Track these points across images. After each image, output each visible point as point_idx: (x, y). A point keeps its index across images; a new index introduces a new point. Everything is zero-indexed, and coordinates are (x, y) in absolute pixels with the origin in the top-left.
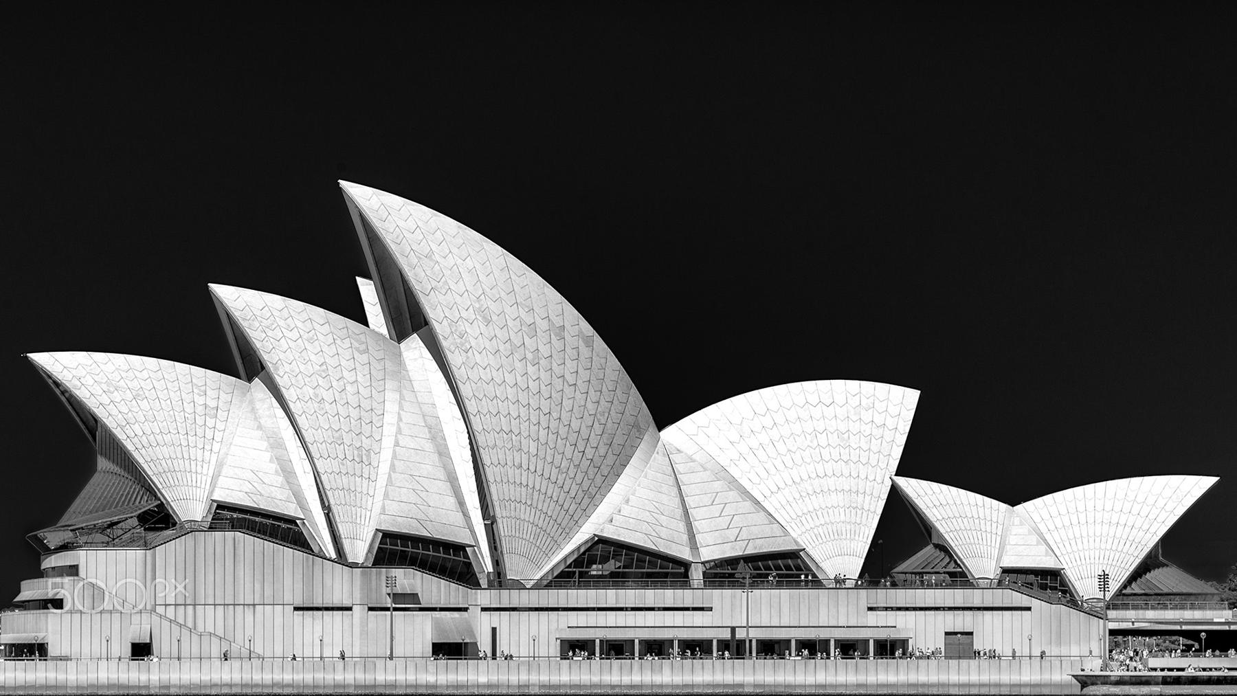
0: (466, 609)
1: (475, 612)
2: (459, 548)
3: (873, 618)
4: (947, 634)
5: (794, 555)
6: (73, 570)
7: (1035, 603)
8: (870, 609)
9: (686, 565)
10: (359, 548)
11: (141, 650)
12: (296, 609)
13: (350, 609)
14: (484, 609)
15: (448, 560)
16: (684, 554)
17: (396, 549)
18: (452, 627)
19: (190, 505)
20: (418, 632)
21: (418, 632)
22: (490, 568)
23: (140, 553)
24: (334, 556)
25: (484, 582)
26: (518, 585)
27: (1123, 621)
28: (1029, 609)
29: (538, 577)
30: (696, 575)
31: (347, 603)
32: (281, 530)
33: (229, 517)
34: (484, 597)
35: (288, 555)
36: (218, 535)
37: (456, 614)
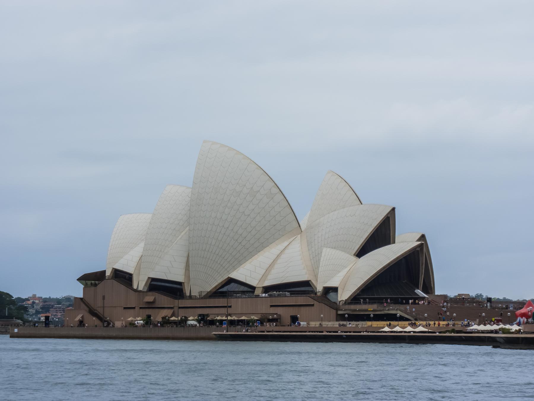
1: (176, 309)
2: (180, 284)
3: (272, 308)
5: (307, 283)
7: (316, 303)
8: (271, 306)
9: (253, 288)
12: (125, 308)
13: (134, 308)
14: (180, 308)
16: (254, 283)
26: (195, 298)
27: (342, 310)
28: (313, 305)
30: (258, 292)
35: (122, 288)
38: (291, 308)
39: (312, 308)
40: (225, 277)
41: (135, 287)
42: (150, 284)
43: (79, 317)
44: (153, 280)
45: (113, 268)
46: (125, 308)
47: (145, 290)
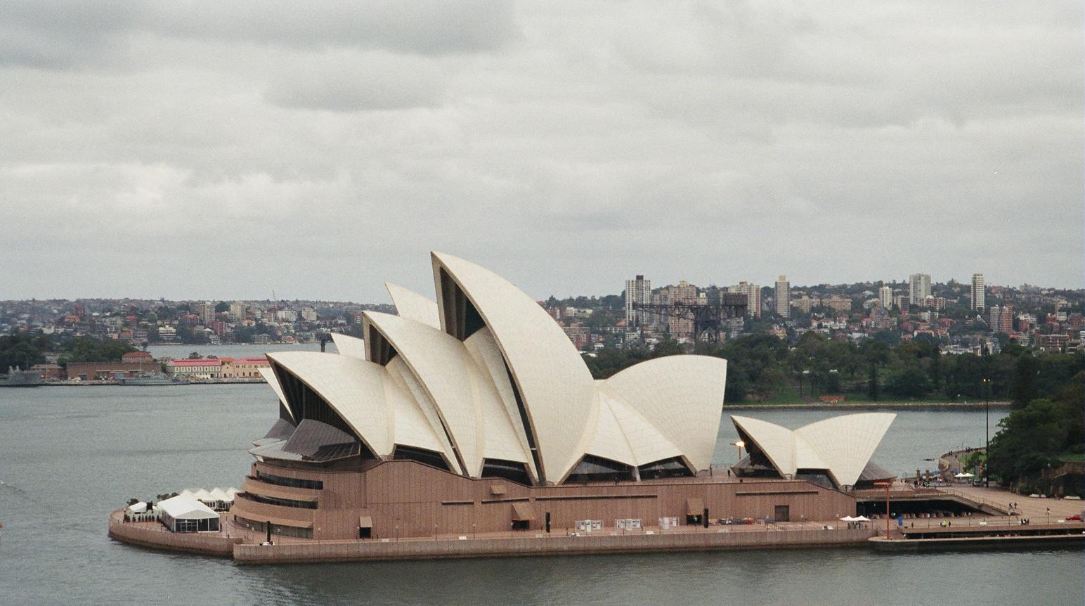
0: (528, 500)
1: (532, 501)
2: (521, 465)
4: (776, 507)
5: (679, 459)
6: (319, 486)
9: (631, 468)
10: (475, 470)
11: (365, 533)
13: (473, 503)
15: (513, 472)
17: (494, 469)
18: (524, 512)
19: (382, 449)
20: (501, 513)
21: (501, 513)
22: (536, 475)
23: (357, 475)
24: (460, 472)
25: (533, 482)
28: (817, 493)
29: (559, 480)
31: (472, 501)
32: (433, 459)
33: (403, 453)
34: (534, 493)
36: (400, 464)
37: (523, 504)
38: (777, 497)
39: (815, 495)
40: (578, 456)
41: (460, 472)
42: (485, 468)
43: (366, 522)
44: (487, 461)
45: (395, 444)
46: (444, 504)
47: (482, 476)
